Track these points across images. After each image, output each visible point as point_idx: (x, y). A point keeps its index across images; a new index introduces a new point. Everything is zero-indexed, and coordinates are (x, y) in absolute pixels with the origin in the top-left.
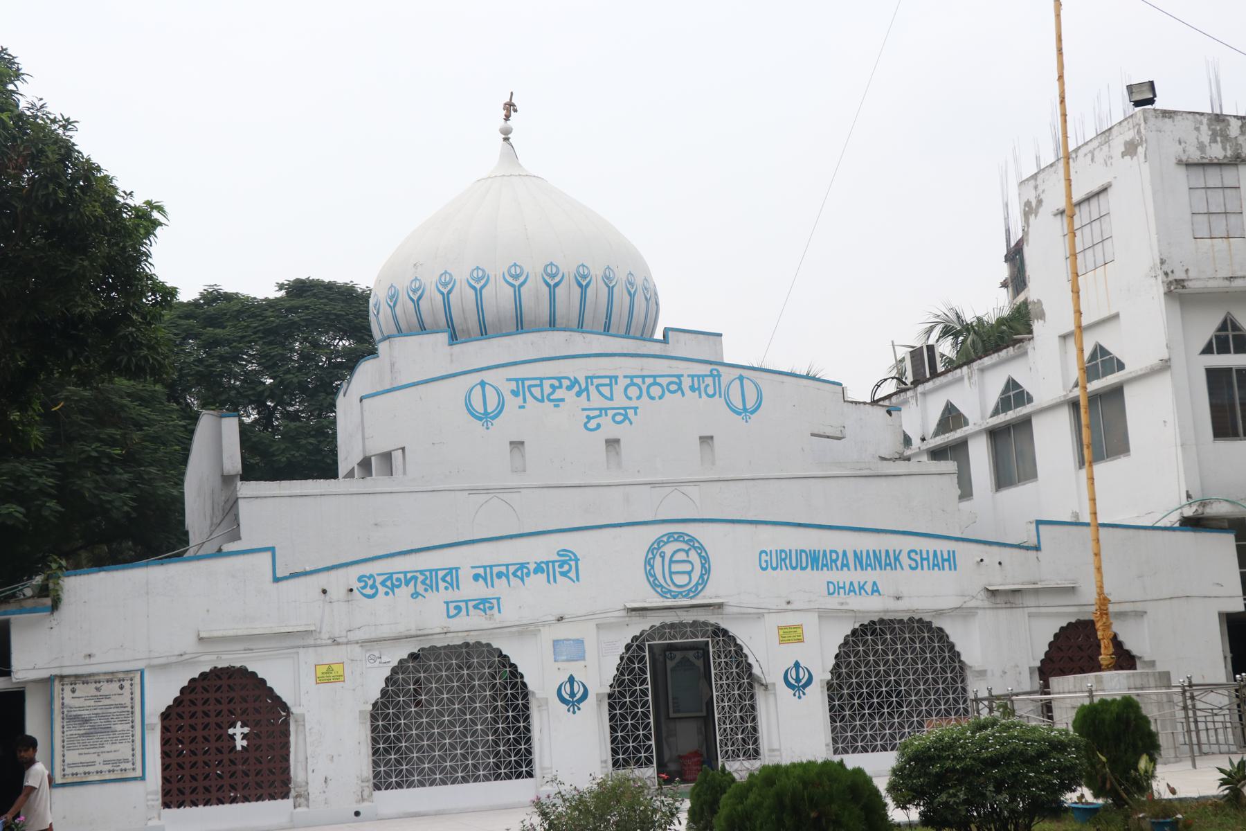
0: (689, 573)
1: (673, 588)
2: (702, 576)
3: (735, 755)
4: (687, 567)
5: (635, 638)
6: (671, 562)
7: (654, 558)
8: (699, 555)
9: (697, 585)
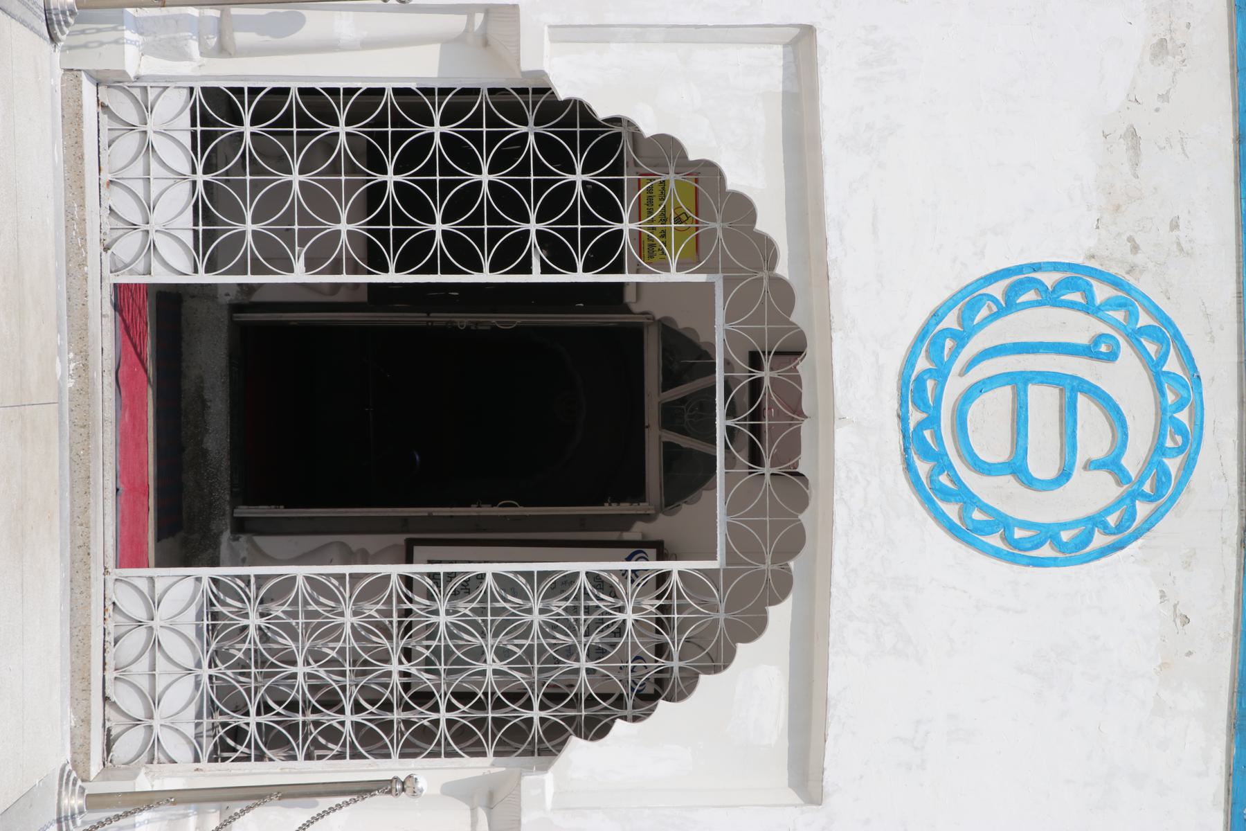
0: (1016, 468)
1: (955, 387)
2: (1003, 523)
3: (215, 624)
4: (1042, 464)
5: (742, 207)
6: (1071, 388)
7: (1089, 308)
8: (1096, 522)
9: (967, 499)
